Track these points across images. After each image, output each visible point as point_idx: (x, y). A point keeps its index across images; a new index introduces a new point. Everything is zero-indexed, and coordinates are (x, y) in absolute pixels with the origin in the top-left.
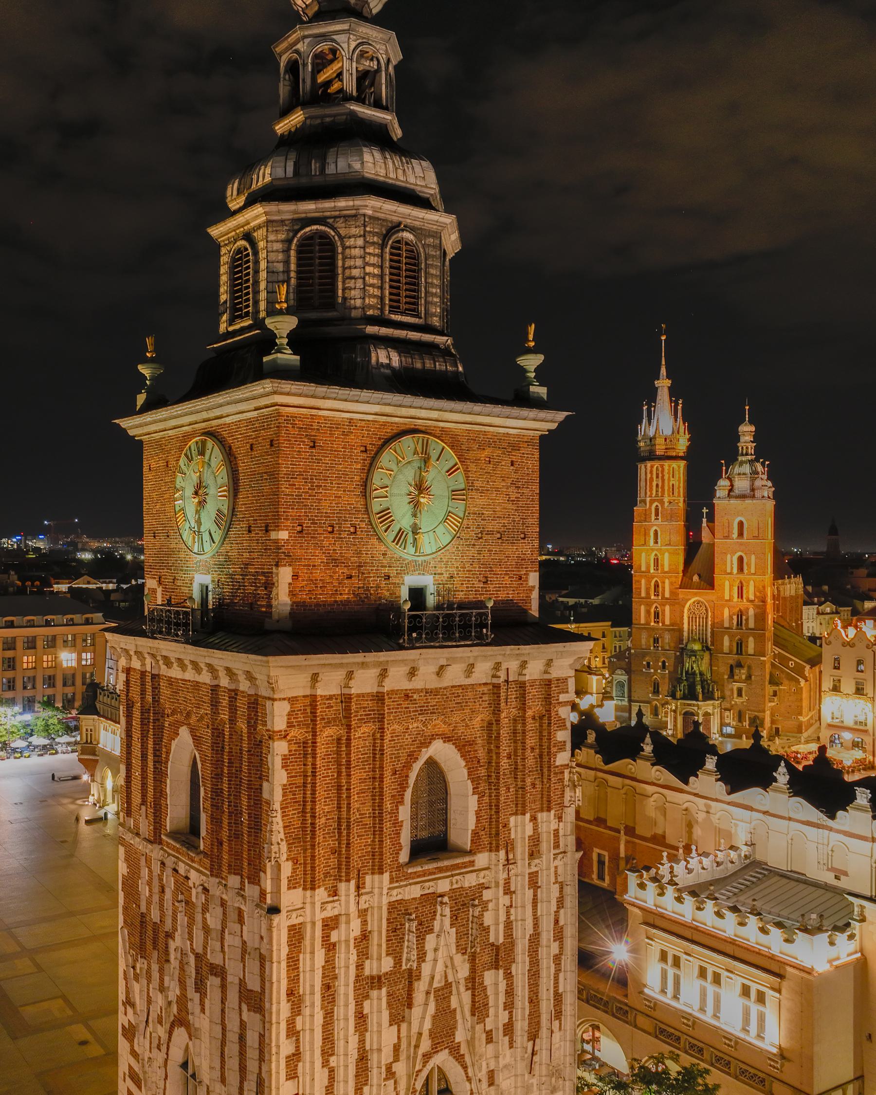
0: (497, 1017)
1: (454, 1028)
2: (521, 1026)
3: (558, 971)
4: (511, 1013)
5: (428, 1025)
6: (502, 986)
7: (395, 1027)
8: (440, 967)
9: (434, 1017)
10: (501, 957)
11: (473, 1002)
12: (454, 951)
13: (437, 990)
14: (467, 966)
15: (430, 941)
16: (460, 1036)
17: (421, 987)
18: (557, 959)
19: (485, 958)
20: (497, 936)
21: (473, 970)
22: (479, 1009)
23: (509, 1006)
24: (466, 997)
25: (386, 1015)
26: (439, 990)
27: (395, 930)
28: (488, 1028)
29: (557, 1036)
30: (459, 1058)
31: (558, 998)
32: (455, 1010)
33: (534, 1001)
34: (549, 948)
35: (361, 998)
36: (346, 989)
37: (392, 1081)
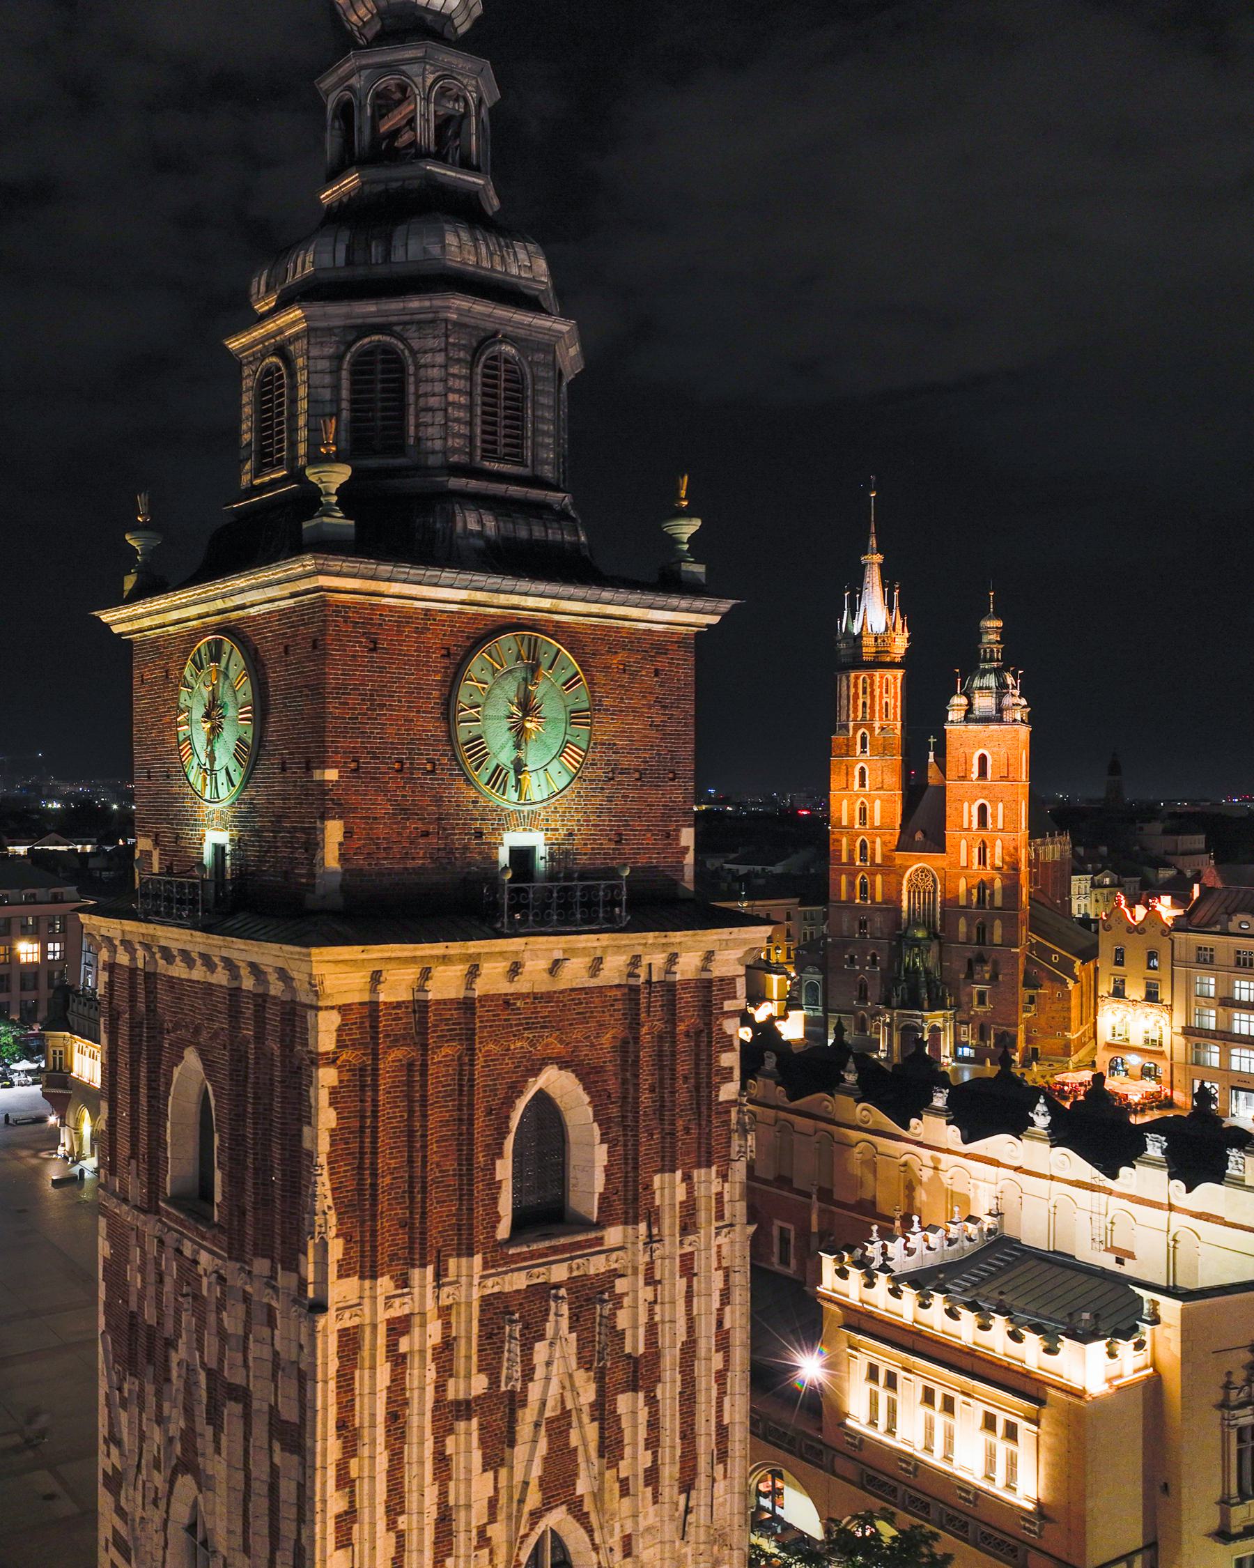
0: (636, 1459)
2: (670, 1472)
3: (722, 1394)
4: (655, 1454)
5: (537, 1471)
6: (643, 1415)
7: (490, 1474)
8: (554, 1388)
9: (546, 1460)
11: (602, 1437)
12: (574, 1366)
13: (550, 1421)
14: (592, 1387)
15: (541, 1351)
16: (583, 1486)
17: (527, 1417)
18: (721, 1376)
19: (619, 1375)
20: (636, 1344)
21: (601, 1392)
22: (610, 1448)
23: (653, 1443)
24: (592, 1430)
25: (477, 1457)
26: (553, 1421)
27: (490, 1336)
28: (622, 1475)
29: (720, 1486)
30: (582, 1518)
31: (723, 1432)
32: (576, 1449)
33: (688, 1435)
34: (709, 1361)
35: (442, 1430)
36: (420, 1418)
37: (486, 1551)
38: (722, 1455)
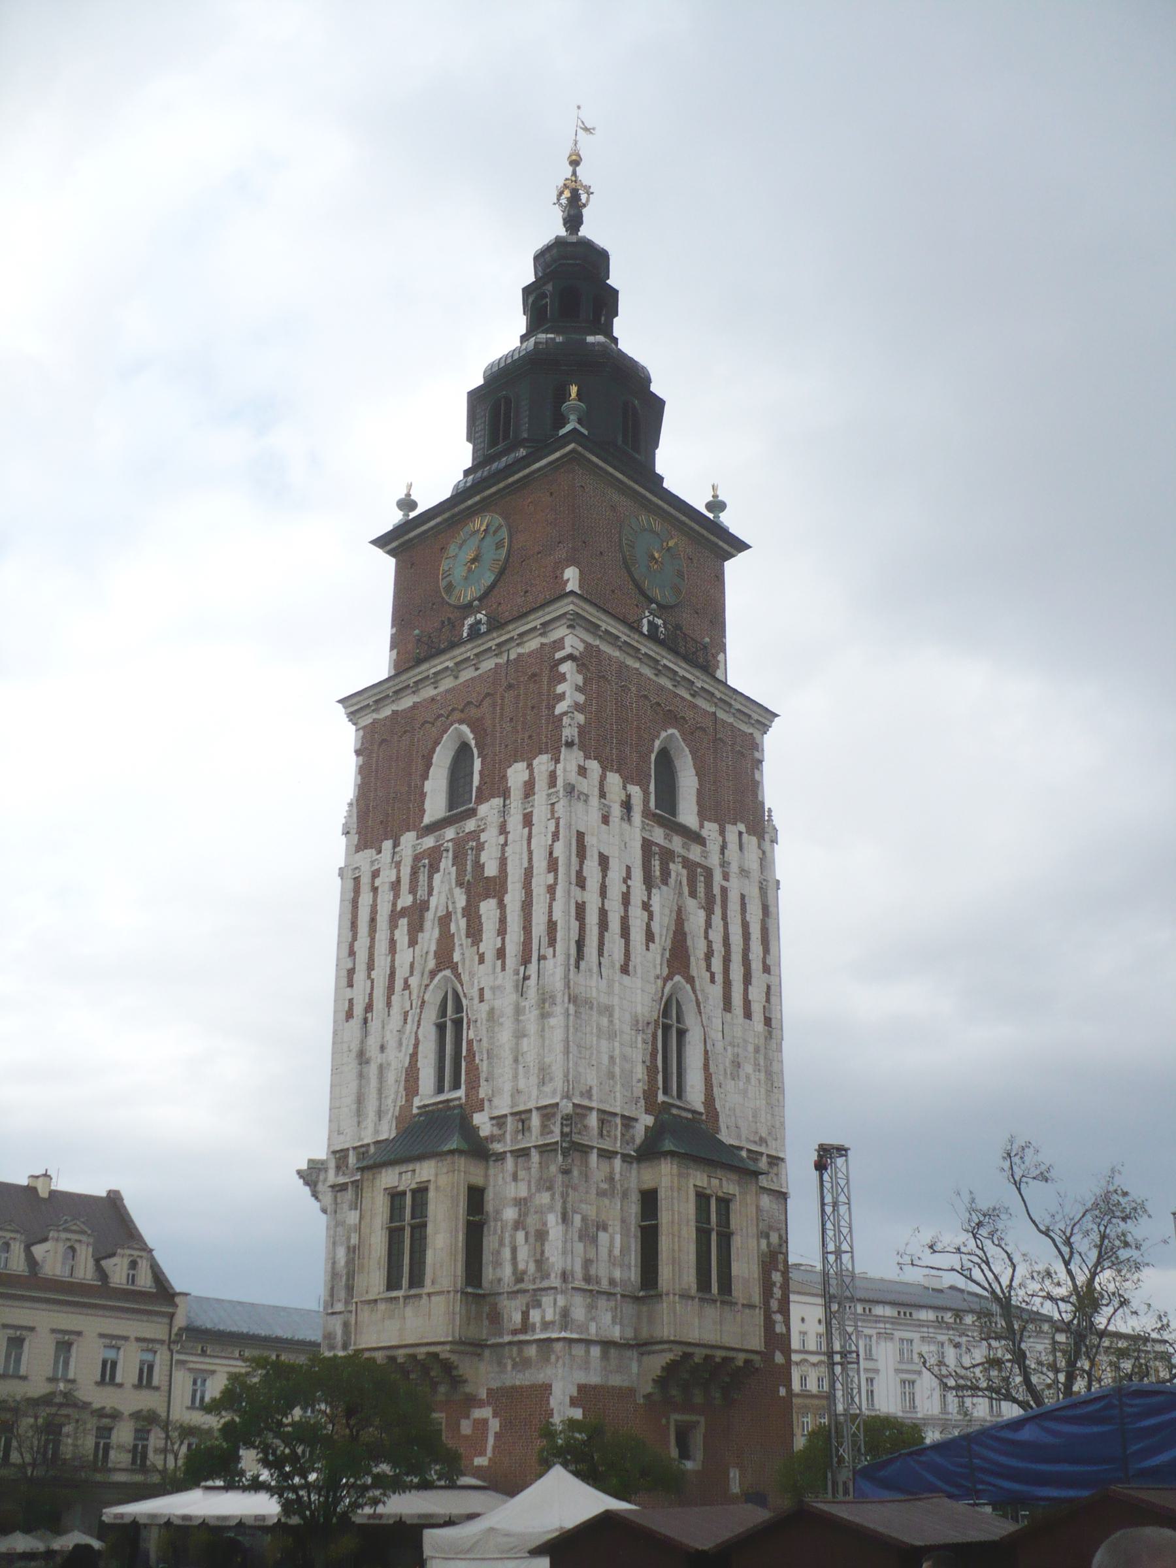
1: (453, 950)
3: (553, 899)
5: (433, 948)
8: (443, 899)
10: (496, 888)
11: (468, 926)
13: (440, 919)
14: (464, 897)
15: (437, 877)
16: (457, 957)
17: (429, 916)
18: (551, 890)
21: (468, 901)
23: (502, 932)
24: (463, 923)
29: (549, 964)
31: (552, 926)
33: (527, 928)
34: (541, 880)
38: (552, 942)
